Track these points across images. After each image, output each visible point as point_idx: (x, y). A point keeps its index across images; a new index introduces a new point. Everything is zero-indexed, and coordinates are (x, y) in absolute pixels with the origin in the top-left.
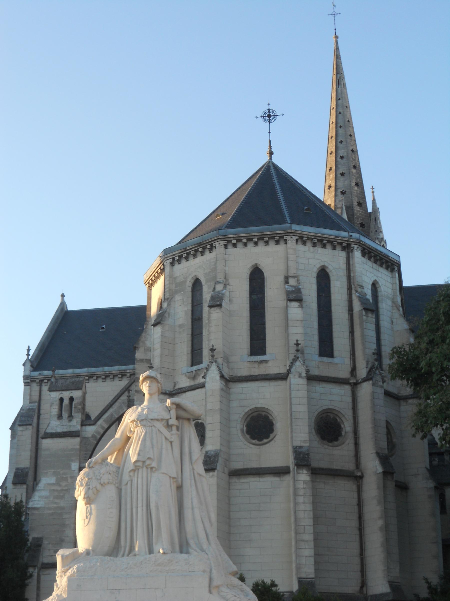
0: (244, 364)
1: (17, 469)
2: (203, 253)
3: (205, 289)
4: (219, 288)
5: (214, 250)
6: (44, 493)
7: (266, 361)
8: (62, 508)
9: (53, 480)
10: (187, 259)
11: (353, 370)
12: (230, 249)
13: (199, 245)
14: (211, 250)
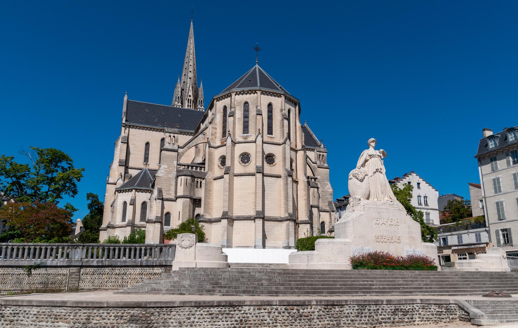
0: (266, 138)
1: (120, 160)
2: (250, 94)
3: (251, 107)
4: (259, 108)
5: (256, 94)
6: (163, 171)
7: (274, 138)
8: (170, 178)
9: (166, 167)
10: (242, 94)
11: (296, 146)
12: (262, 96)
13: (250, 90)
14: (254, 93)
